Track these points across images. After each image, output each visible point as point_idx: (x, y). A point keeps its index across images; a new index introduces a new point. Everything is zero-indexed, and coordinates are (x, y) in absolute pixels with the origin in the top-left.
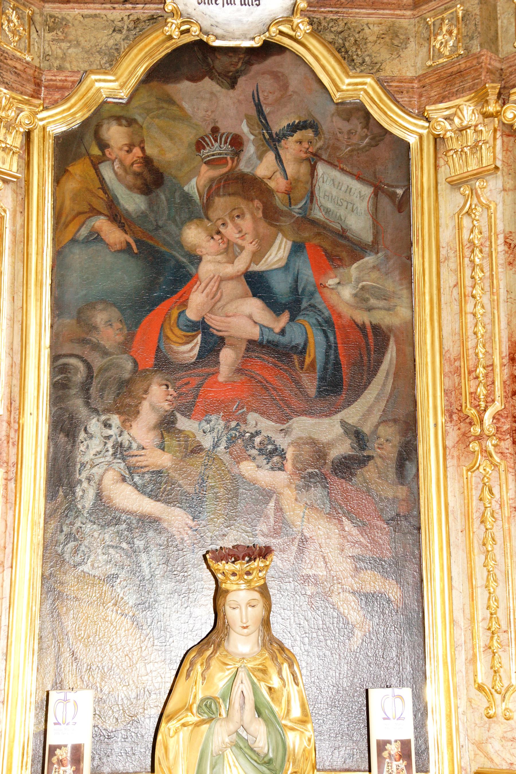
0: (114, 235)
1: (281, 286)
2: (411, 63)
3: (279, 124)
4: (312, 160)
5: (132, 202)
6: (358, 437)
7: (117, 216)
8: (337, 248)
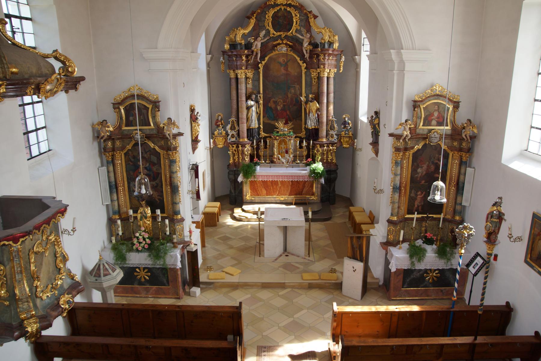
0: (131, 164)
1: (148, 168)
2: (160, 145)
3: (147, 150)
4: (150, 155)
5: (132, 160)
6: (157, 184)
7: (131, 162)
8: (154, 164)
